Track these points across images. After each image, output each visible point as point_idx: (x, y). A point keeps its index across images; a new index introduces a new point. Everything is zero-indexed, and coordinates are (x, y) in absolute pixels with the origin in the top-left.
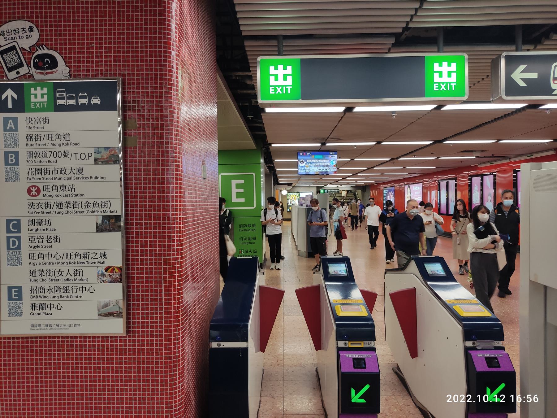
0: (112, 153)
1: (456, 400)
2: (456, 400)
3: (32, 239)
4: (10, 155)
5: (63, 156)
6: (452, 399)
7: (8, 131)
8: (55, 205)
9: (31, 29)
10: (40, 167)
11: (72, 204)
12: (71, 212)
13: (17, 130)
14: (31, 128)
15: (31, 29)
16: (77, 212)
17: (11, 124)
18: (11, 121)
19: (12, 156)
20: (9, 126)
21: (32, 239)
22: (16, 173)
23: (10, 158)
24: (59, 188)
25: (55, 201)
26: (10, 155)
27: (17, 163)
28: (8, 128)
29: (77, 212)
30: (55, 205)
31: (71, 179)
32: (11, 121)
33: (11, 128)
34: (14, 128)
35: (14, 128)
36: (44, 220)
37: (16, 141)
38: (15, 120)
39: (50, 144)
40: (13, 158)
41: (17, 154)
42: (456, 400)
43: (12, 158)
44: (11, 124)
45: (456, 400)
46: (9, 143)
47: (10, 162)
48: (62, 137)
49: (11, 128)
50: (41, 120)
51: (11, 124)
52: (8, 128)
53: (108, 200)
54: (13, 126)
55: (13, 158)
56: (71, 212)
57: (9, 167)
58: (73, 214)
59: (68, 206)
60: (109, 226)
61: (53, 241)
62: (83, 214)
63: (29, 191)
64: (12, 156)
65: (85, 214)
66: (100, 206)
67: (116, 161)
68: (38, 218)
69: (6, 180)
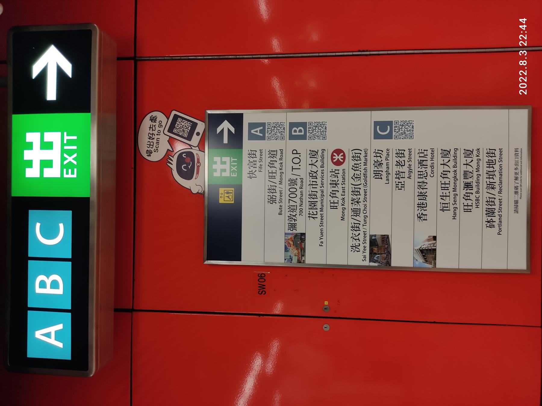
0: (292, 243)
1: (524, 86)
2: (525, 86)
3: (400, 186)
4: (293, 134)
5: (295, 186)
6: (524, 90)
7: (264, 135)
8: (355, 217)
9: (153, 119)
10: (308, 203)
11: (355, 197)
12: (365, 206)
13: (263, 124)
14: (261, 165)
15: (153, 119)
16: (365, 200)
17: (257, 131)
18: (252, 131)
19: (295, 131)
20: (258, 134)
21: (400, 186)
22: (316, 127)
23: (298, 133)
24: (334, 189)
25: (350, 217)
26: (293, 134)
27: (304, 125)
28: (261, 135)
29: (365, 200)
30: (355, 217)
31: (322, 192)
32: (252, 131)
33: (261, 131)
34: (261, 128)
35: (261, 128)
36: (376, 159)
37: (277, 125)
38: (252, 126)
39: (280, 186)
40: (298, 130)
41: (292, 125)
42: (524, 86)
43: (297, 131)
44: (256, 131)
45: (525, 86)
46: (279, 134)
47: (303, 133)
48: (272, 159)
49: (261, 131)
50: (252, 160)
51: (257, 131)
52: (261, 135)
53: (351, 152)
54: (258, 129)
55: (298, 130)
56: (365, 206)
57: (308, 134)
58: (368, 204)
59: (358, 202)
60: (381, 254)
61: (403, 159)
62: (368, 191)
63: (338, 151)
64: (295, 131)
65: (368, 188)
66: (359, 162)
67: (301, 239)
68: (373, 166)
69: (324, 138)
